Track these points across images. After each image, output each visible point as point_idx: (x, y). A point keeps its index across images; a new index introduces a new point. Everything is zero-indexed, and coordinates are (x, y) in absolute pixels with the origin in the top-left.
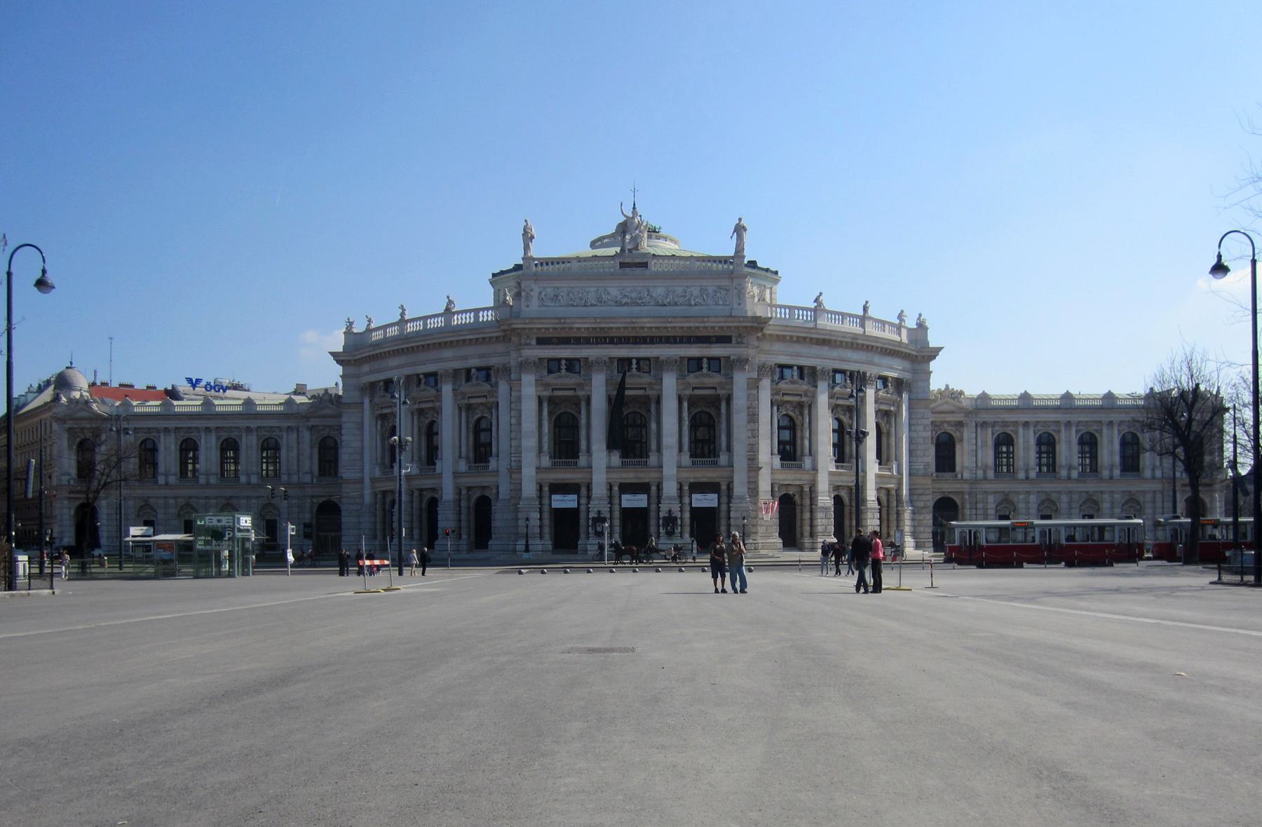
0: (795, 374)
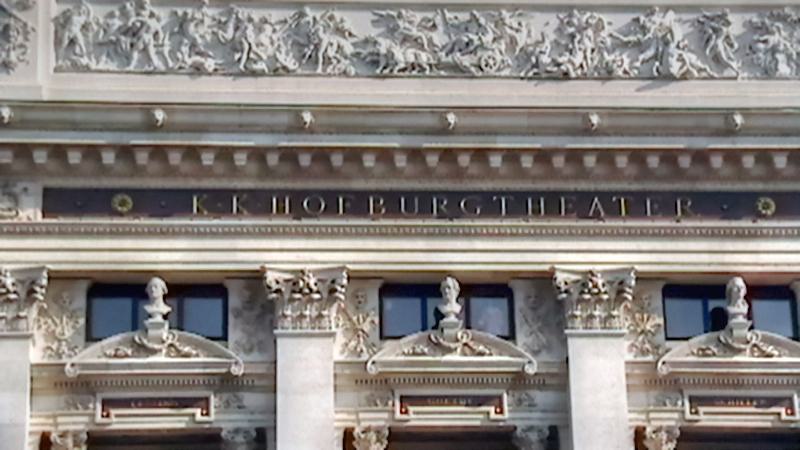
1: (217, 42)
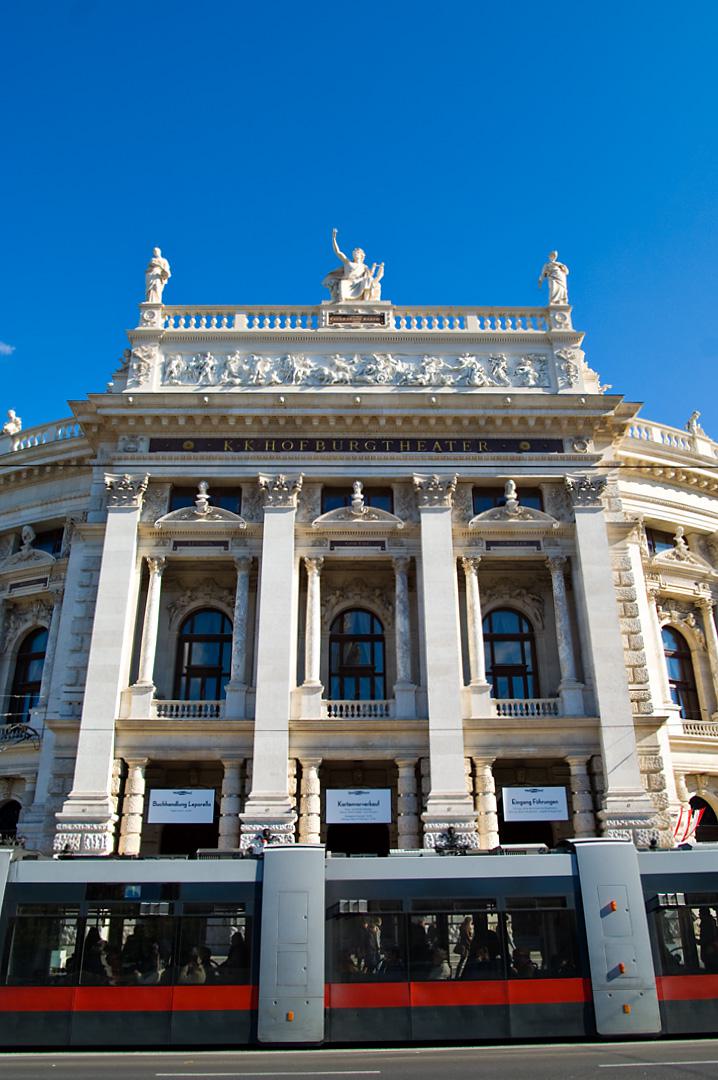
0: (680, 540)
1: (241, 372)
